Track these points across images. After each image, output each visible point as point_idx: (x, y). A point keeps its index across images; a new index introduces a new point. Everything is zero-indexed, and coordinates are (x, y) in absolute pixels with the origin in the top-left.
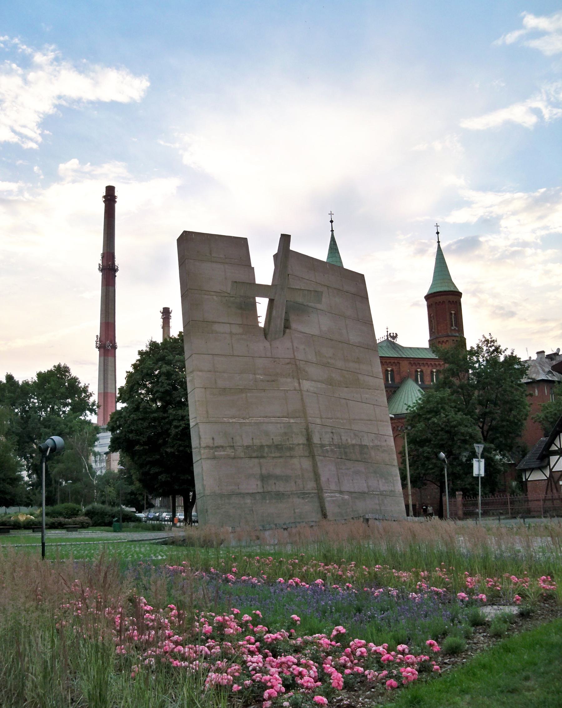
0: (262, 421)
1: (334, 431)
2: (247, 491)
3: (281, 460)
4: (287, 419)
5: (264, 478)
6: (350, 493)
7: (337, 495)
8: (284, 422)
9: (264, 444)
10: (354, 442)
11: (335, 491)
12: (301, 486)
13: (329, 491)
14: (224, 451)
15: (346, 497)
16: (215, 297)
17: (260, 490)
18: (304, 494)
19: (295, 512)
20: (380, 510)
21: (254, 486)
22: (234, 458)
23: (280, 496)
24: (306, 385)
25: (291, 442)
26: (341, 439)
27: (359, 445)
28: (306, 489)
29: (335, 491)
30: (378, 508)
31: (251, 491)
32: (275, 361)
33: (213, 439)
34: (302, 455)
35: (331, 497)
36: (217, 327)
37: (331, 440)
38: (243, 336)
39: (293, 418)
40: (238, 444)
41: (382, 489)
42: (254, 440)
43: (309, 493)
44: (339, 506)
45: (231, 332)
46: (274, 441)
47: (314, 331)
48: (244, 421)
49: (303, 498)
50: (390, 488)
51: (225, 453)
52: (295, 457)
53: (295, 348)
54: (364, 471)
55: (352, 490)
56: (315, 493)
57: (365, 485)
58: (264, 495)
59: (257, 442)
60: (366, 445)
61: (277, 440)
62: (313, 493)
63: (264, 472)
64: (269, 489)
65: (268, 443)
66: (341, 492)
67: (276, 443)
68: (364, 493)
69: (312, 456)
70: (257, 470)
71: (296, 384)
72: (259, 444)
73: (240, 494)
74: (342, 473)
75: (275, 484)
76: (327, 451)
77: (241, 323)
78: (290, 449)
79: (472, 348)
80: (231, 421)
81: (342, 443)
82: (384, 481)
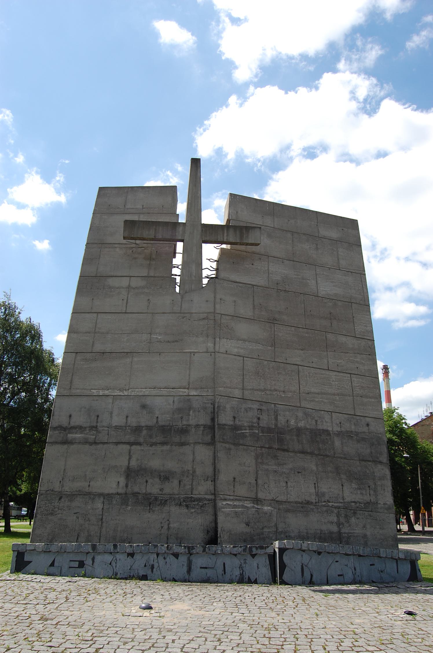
0: (147, 393)
1: (263, 408)
2: (100, 491)
3: (166, 448)
4: (186, 390)
5: (130, 473)
6: (276, 502)
7: (248, 504)
8: (181, 394)
9: (143, 424)
10: (301, 424)
11: (247, 499)
12: (188, 487)
13: (232, 498)
14: (81, 433)
15: (266, 508)
16: (118, 250)
17: (121, 491)
18: (192, 500)
19: (169, 528)
20: (340, 533)
21: (113, 483)
22: (95, 443)
23: (150, 502)
24: (225, 345)
25: (185, 423)
26: (276, 419)
27: (311, 430)
28: (195, 492)
29: (247, 499)
30: (335, 529)
31: (106, 491)
32: (183, 318)
33: (70, 416)
34: (200, 441)
35: (235, 506)
36: (111, 282)
37: (255, 420)
38: (146, 290)
39: (196, 389)
40: (105, 424)
41: (348, 499)
42: (129, 419)
43: (199, 500)
44: (248, 524)
45: (129, 285)
46: (159, 419)
47: (259, 280)
48: (121, 394)
49: (187, 506)
50: (367, 498)
51: (83, 435)
52: (188, 444)
53: (218, 300)
54: (314, 468)
55: (282, 498)
56: (209, 500)
57: (313, 490)
58: (125, 498)
59: (133, 422)
60: (327, 431)
61: (164, 419)
62: (206, 499)
63: (134, 463)
64: (136, 489)
65: (150, 423)
66: (257, 500)
67: (161, 423)
68: (308, 503)
69: (268, 448)
70: (123, 462)
71: (210, 345)
72: (134, 424)
73: (89, 493)
74: (267, 470)
75: (147, 482)
76: (243, 436)
77: (146, 274)
78: (184, 431)
79: (219, 152)
80: (101, 393)
81: (276, 425)
82: (354, 486)
